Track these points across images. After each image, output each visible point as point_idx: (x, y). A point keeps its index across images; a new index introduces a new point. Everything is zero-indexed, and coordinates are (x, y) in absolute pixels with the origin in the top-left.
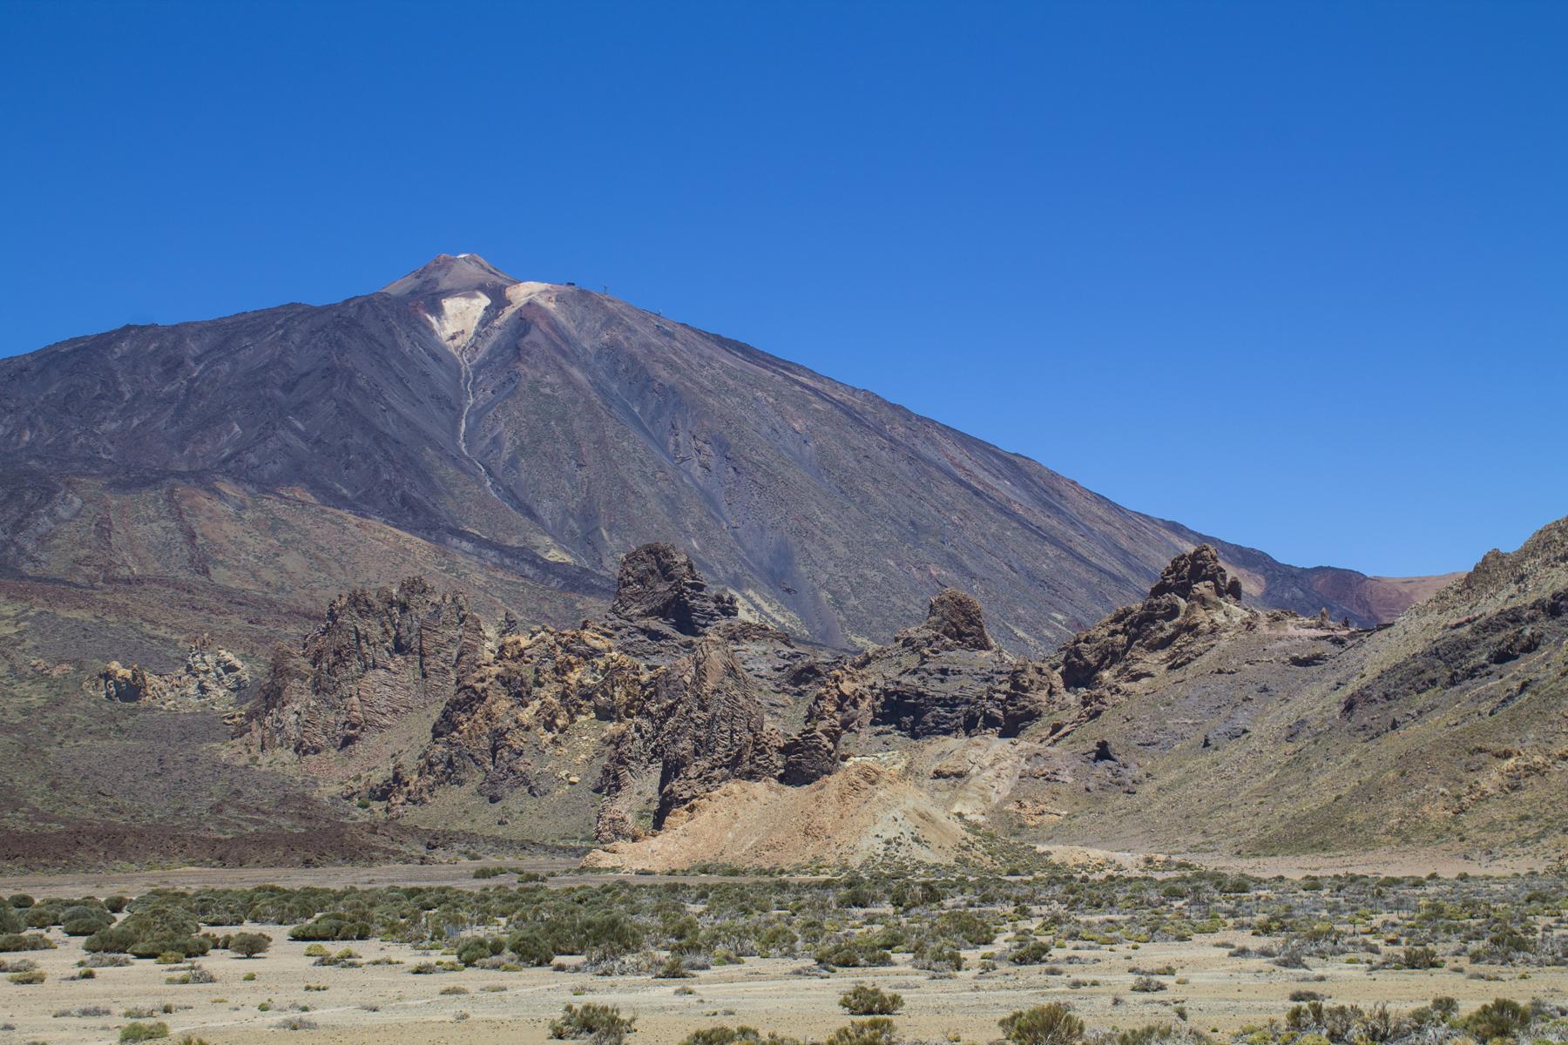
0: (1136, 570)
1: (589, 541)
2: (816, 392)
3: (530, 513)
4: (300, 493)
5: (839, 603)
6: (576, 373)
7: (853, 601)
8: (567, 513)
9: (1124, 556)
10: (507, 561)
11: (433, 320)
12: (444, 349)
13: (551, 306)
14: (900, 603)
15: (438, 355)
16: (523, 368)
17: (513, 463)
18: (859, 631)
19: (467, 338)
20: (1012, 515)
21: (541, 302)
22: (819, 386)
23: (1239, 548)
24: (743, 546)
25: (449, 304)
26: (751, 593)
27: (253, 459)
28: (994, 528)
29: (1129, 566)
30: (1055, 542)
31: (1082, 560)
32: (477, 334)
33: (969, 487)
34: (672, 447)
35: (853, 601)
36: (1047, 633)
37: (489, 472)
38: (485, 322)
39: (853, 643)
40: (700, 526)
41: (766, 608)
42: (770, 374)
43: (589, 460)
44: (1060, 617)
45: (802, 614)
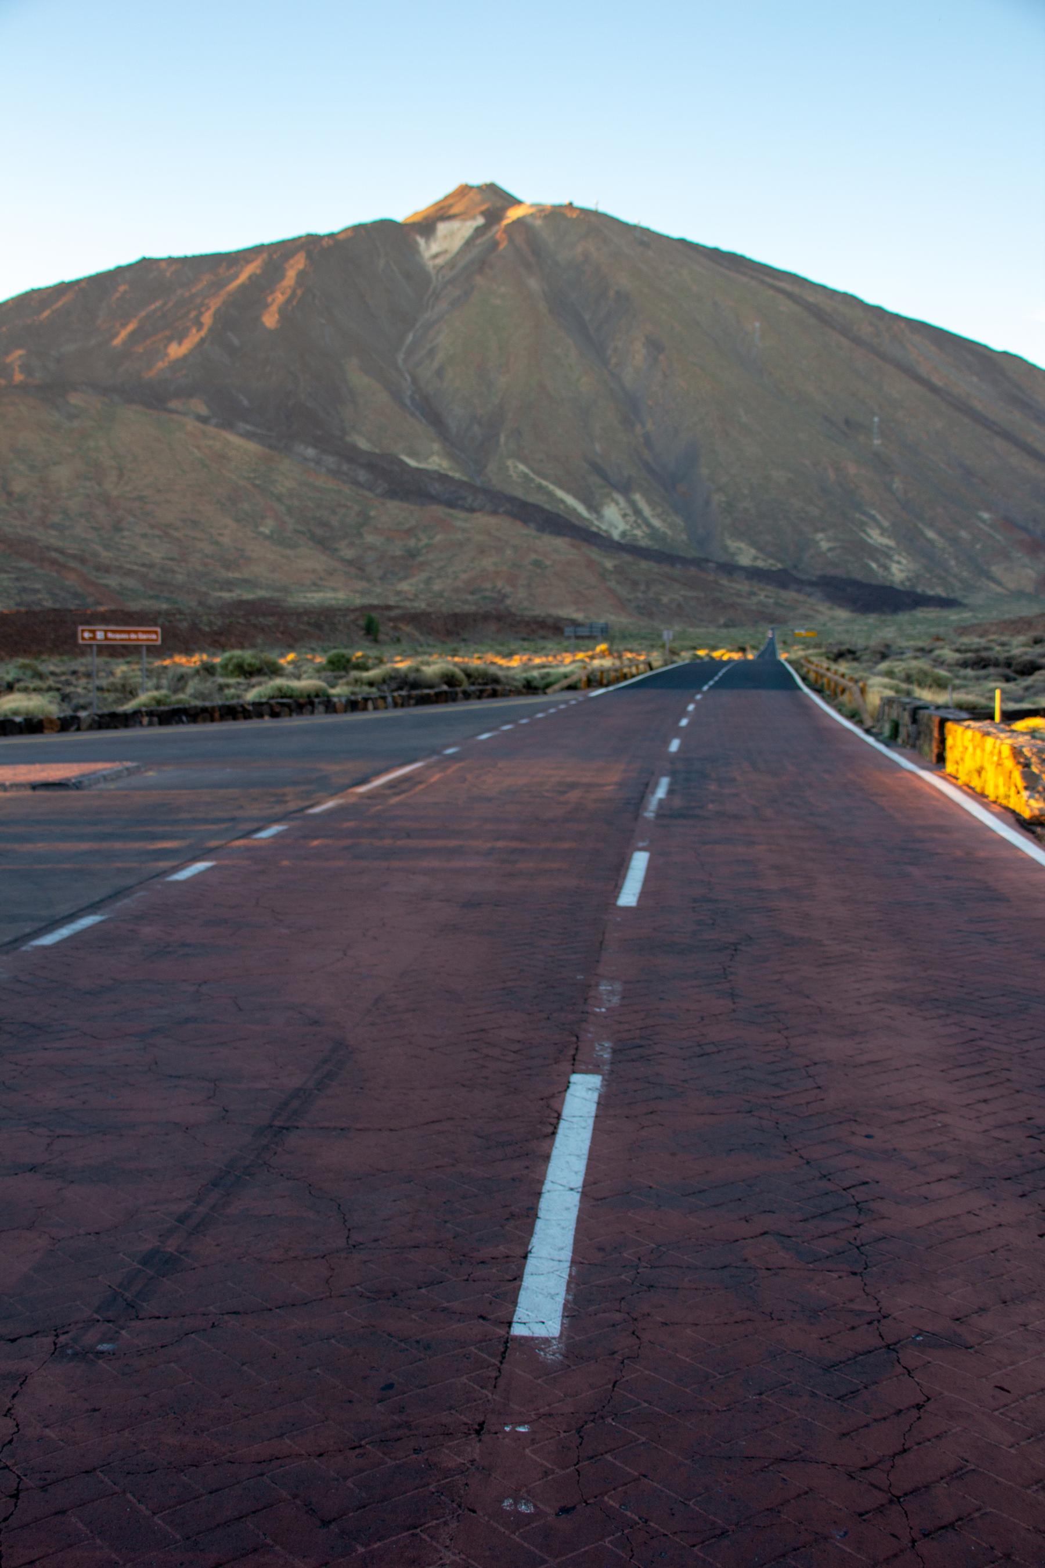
2: (790, 296)
6: (534, 284)
10: (345, 467)
11: (421, 241)
12: (422, 269)
13: (538, 223)
15: (415, 274)
16: (479, 280)
17: (440, 373)
18: (739, 535)
19: (448, 257)
21: (529, 220)
22: (796, 290)
25: (442, 228)
26: (637, 497)
30: (1007, 436)
32: (458, 253)
34: (609, 352)
36: (963, 534)
38: (469, 243)
41: (647, 511)
42: (745, 279)
44: (986, 516)
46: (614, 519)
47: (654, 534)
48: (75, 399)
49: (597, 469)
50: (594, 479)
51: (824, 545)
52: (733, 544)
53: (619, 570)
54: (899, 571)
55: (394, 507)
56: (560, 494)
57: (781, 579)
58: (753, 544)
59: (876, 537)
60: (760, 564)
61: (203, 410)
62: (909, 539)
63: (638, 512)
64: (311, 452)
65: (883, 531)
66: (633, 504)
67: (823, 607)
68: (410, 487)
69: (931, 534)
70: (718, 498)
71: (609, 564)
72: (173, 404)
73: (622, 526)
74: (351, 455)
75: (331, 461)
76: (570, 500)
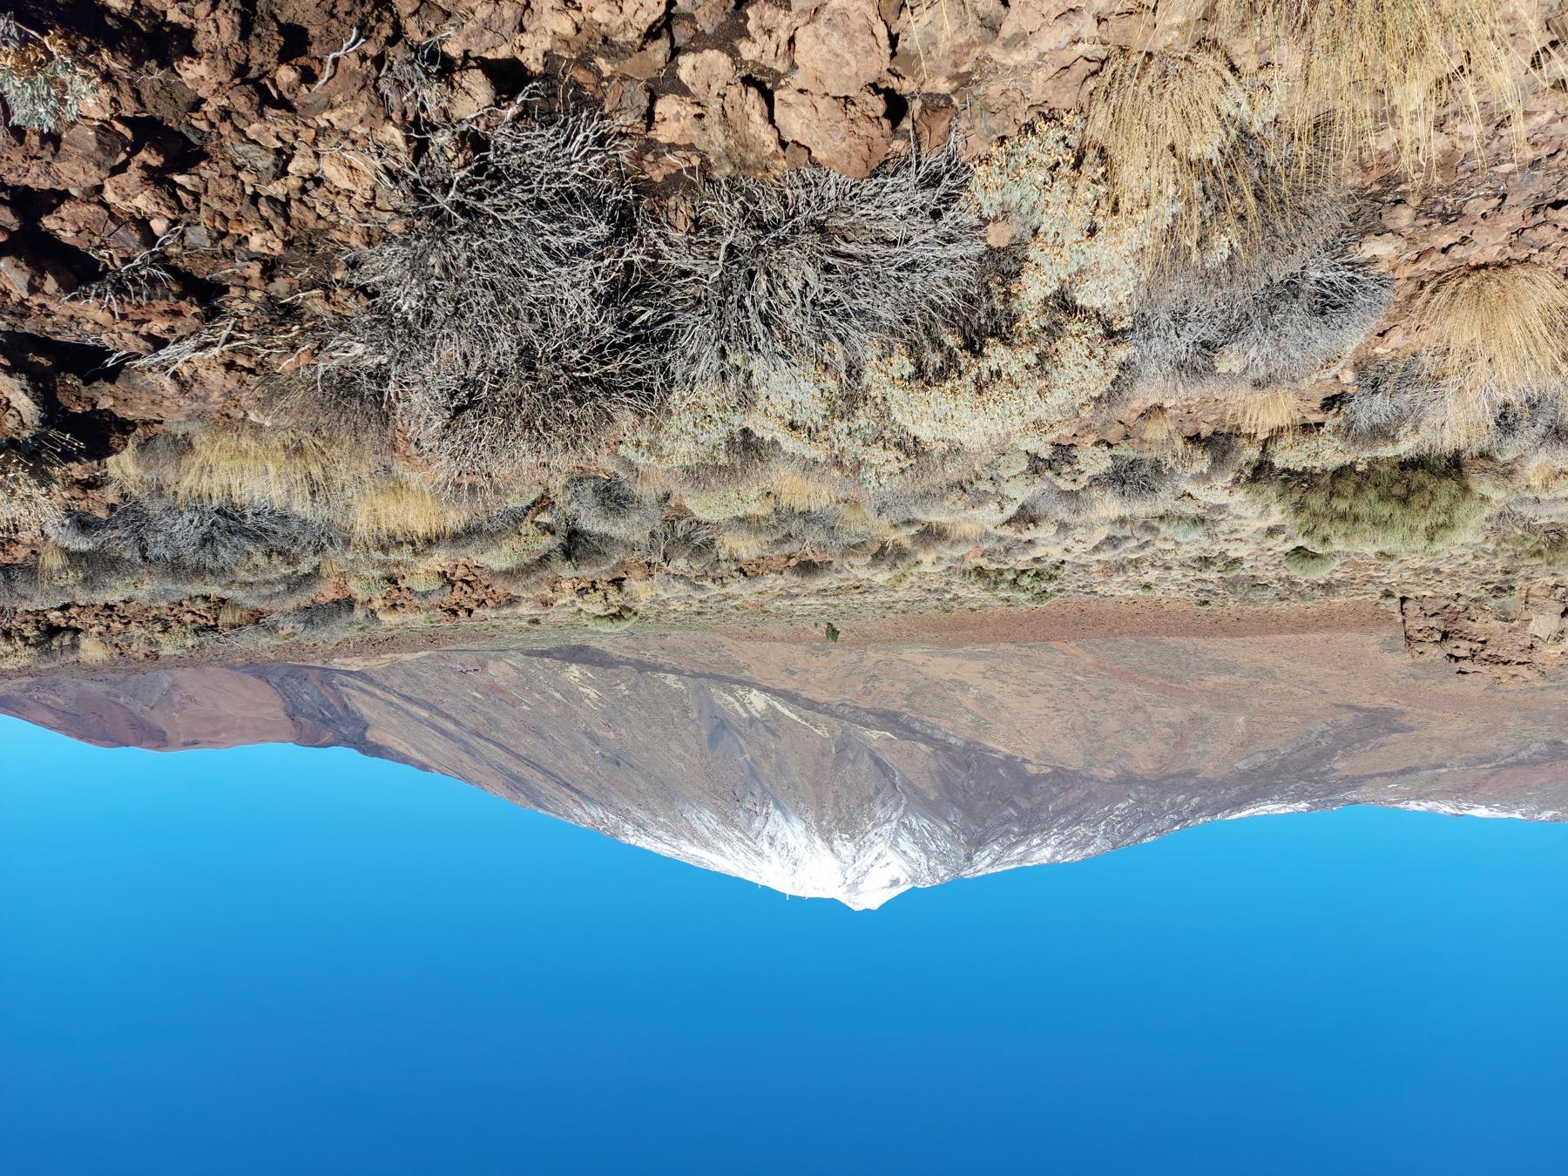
0: (461, 741)
1: (843, 746)
3: (877, 761)
4: (1032, 769)
5: (686, 710)
7: (675, 713)
8: (853, 762)
9: (468, 749)
14: (643, 713)
17: (878, 791)
20: (546, 772)
23: (381, 756)
24: (740, 746)
27: (1054, 790)
28: (561, 764)
29: (465, 743)
30: (518, 757)
31: (500, 746)
33: (573, 789)
35: (675, 713)
37: (894, 786)
39: (685, 684)
40: (767, 756)
41: (737, 705)
43: (831, 796)
45: (711, 702)
46: (758, 701)
47: (731, 692)
48: (1111, 773)
49: (773, 733)
50: (774, 726)
51: (622, 687)
52: (680, 685)
53: (741, 670)
54: (574, 672)
55: (893, 708)
56: (793, 716)
57: (641, 666)
58: (667, 687)
59: (591, 692)
60: (662, 675)
61: (1028, 767)
62: (570, 693)
63: (743, 705)
64: (952, 741)
65: (587, 697)
66: (747, 711)
67: (609, 649)
68: (889, 719)
69: (558, 695)
70: (694, 715)
71: (746, 673)
72: (1049, 770)
73: (751, 696)
74: (928, 740)
75: (938, 735)
76: (786, 712)
